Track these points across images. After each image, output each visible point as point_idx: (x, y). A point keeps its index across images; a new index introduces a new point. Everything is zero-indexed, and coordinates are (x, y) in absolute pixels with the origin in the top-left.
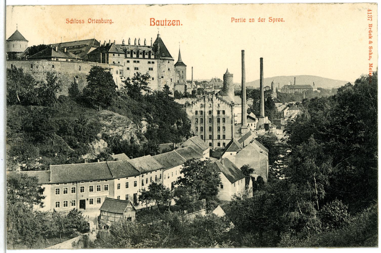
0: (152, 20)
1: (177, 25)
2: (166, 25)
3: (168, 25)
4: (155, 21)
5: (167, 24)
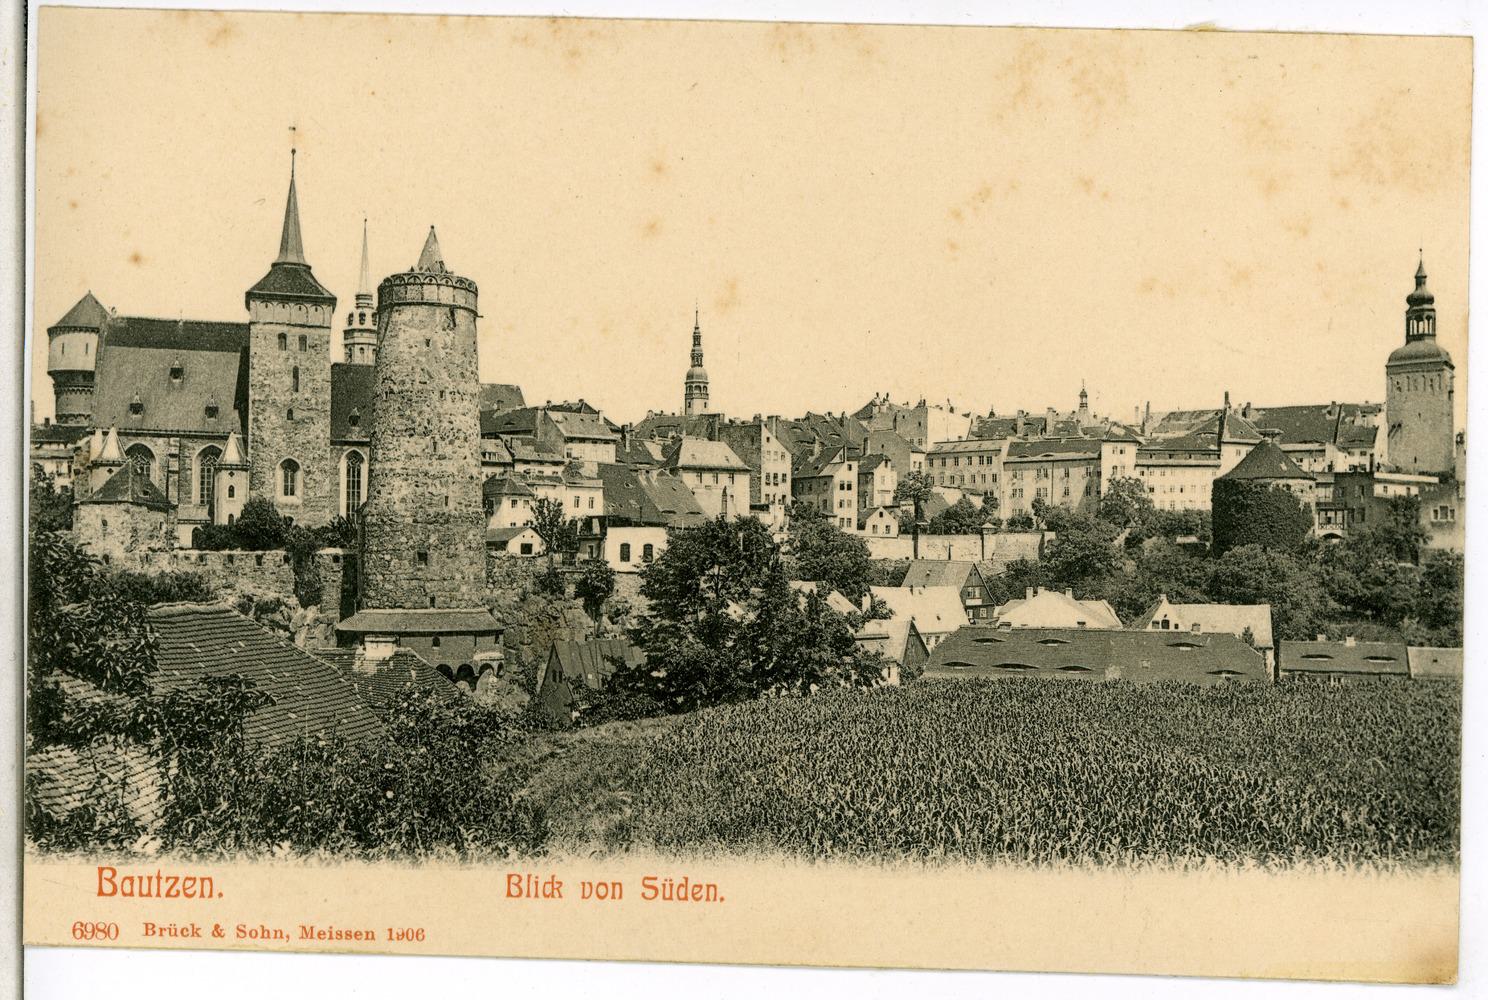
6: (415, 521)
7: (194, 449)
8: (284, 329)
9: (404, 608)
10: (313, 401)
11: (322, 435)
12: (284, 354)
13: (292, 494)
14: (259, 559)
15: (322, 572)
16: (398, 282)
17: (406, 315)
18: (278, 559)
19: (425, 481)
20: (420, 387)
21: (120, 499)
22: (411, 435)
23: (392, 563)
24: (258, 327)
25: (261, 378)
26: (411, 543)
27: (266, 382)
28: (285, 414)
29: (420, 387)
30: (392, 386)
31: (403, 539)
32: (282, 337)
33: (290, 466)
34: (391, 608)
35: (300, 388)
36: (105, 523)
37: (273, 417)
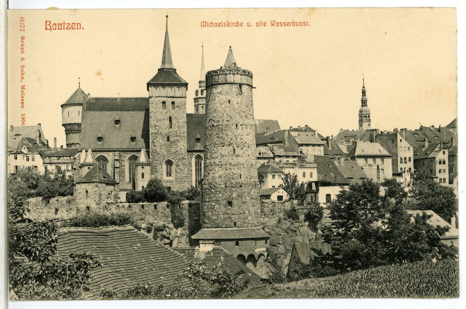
0: (48, 23)
1: (77, 29)
2: (64, 29)
3: (67, 29)
4: (51, 25)
5: (65, 28)
6: (226, 186)
7: (126, 156)
8: (164, 99)
9: (222, 228)
10: (179, 132)
11: (183, 148)
12: (165, 111)
13: (170, 176)
14: (155, 206)
16: (215, 74)
17: (219, 89)
19: (230, 167)
20: (227, 123)
21: (93, 181)
23: (216, 207)
24: (153, 99)
25: (155, 123)
26: (224, 197)
27: (157, 124)
28: (166, 139)
29: (227, 123)
30: (213, 123)
31: (221, 195)
32: (164, 103)
33: (169, 163)
34: (215, 228)
35: (172, 126)
36: (87, 192)
37: (161, 140)
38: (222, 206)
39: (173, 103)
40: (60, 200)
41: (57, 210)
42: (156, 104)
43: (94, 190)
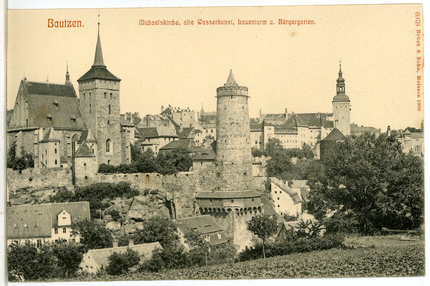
8: (106, 91)
10: (115, 117)
12: (106, 100)
15: (182, 180)
18: (155, 176)
21: (91, 155)
22: (241, 137)
23: (237, 176)
27: (101, 110)
28: (107, 122)
29: (243, 121)
30: (233, 121)
36: (85, 164)
37: (104, 123)
38: (241, 176)
39: (111, 94)
40: (33, 171)
41: (31, 180)
42: (100, 94)
43: (92, 164)
